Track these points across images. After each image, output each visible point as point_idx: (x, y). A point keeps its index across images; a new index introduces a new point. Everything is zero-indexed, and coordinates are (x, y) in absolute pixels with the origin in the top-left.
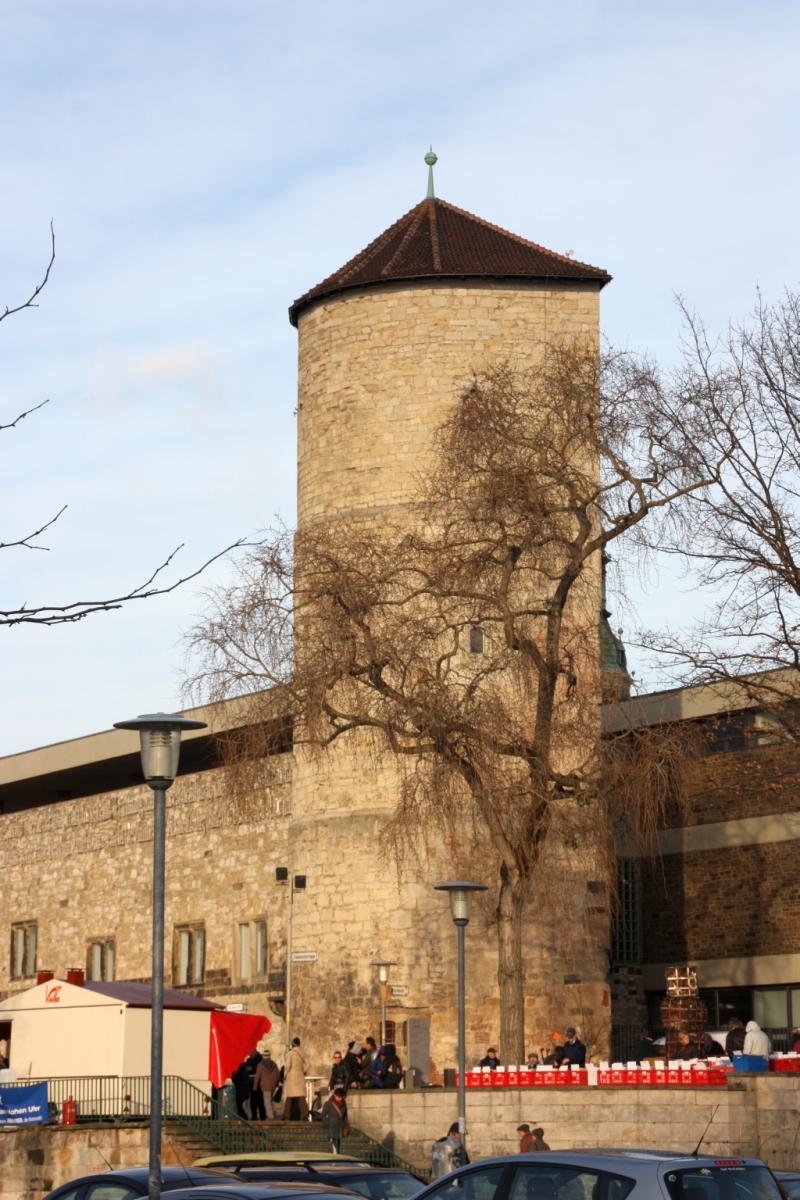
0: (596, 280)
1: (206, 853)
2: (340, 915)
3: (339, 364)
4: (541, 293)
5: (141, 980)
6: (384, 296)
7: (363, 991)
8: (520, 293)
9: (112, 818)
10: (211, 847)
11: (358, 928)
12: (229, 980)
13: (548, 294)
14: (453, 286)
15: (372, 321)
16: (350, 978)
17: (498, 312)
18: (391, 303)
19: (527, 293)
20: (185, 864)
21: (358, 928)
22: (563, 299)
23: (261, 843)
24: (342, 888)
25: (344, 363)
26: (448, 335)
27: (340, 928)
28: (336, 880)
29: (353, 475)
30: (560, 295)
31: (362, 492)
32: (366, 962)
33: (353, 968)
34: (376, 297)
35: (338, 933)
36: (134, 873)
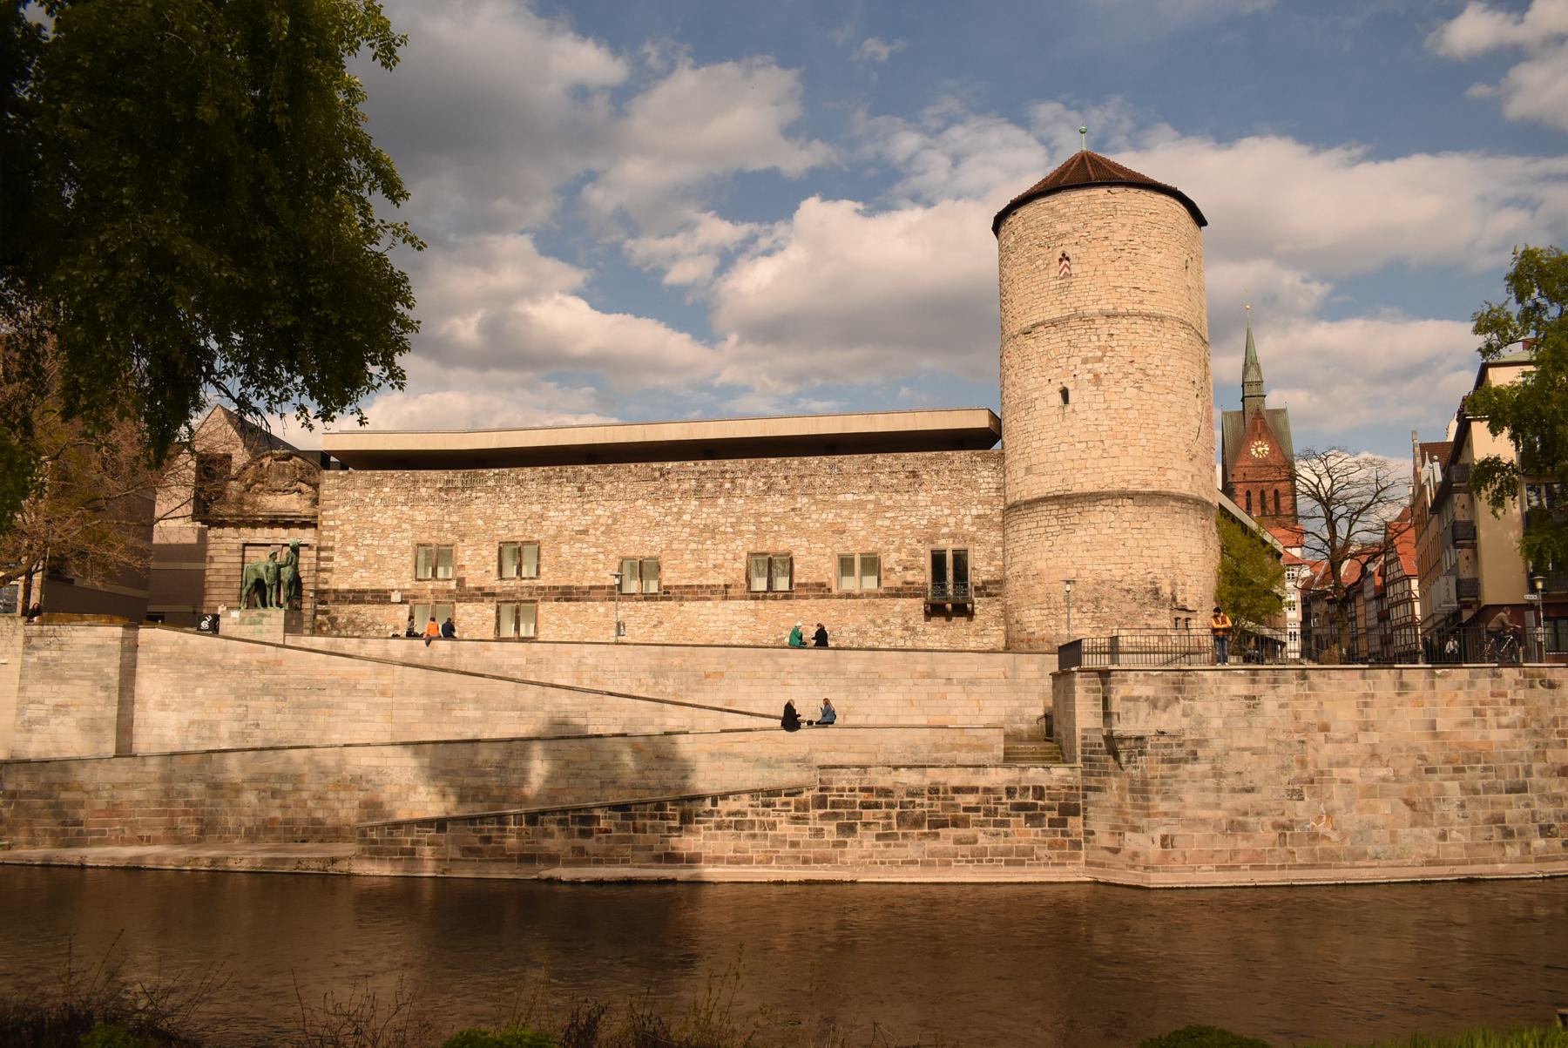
0: (1200, 221)
1: (793, 510)
2: (1146, 552)
3: (1124, 225)
5: (700, 587)
6: (1153, 195)
7: (1166, 600)
9: (655, 479)
10: (799, 505)
11: (1161, 561)
12: (829, 590)
16: (1156, 592)
20: (765, 514)
21: (1161, 561)
23: (870, 506)
24: (1148, 536)
25: (1129, 227)
27: (1148, 560)
28: (1143, 531)
29: (1138, 292)
32: (1167, 582)
33: (1158, 585)
34: (1148, 194)
35: (1146, 564)
36: (687, 517)
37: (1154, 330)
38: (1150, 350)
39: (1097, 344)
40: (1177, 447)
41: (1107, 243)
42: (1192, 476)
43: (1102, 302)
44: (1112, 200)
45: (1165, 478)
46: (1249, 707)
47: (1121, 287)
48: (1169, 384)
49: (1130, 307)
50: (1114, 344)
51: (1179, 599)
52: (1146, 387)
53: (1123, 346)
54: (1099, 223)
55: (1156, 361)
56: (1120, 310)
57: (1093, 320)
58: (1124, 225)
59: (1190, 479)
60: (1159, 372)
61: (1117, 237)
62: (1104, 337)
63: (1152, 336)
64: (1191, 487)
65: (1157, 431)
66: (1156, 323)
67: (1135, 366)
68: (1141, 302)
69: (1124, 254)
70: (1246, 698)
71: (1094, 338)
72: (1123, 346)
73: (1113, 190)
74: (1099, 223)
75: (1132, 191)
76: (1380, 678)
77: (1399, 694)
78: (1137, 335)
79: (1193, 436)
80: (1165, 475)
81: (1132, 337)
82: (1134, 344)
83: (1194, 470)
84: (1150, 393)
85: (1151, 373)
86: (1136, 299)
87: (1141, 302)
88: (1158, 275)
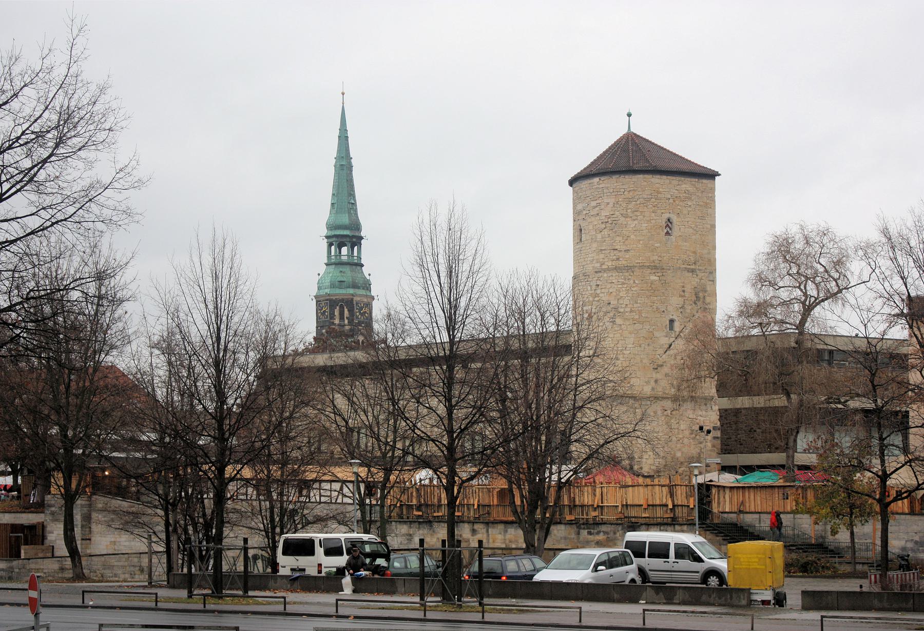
0: (711, 175)
3: (608, 204)
4: (694, 180)
8: (687, 179)
13: (697, 180)
14: (661, 175)
15: (624, 187)
17: (679, 186)
18: (633, 180)
19: (689, 179)
22: (702, 183)
25: (611, 205)
26: (659, 195)
30: (701, 181)
31: (621, 259)
34: (627, 177)
37: (625, 279)
38: (621, 294)
39: (590, 292)
40: (641, 361)
41: (598, 218)
42: (656, 381)
43: (594, 262)
44: (601, 186)
45: (629, 385)
46: (408, 540)
47: (605, 250)
48: (637, 317)
49: (610, 264)
50: (598, 291)
51: (636, 467)
52: (619, 321)
53: (604, 293)
54: (593, 204)
55: (626, 301)
56: (604, 267)
57: (589, 276)
58: (608, 204)
59: (652, 383)
60: (629, 310)
61: (604, 213)
62: (594, 287)
63: (623, 284)
64: (653, 389)
65: (625, 352)
66: (627, 274)
67: (612, 306)
68: (618, 259)
69: (608, 225)
70: (407, 535)
71: (589, 288)
72: (604, 293)
73: (603, 178)
74: (593, 204)
75: (615, 177)
76: (464, 527)
77: (472, 535)
78: (613, 284)
79: (661, 351)
80: (629, 383)
81: (609, 286)
82: (611, 291)
83: (659, 376)
84: (620, 325)
85: (622, 310)
86: (614, 257)
87: (618, 259)
88: (632, 237)
